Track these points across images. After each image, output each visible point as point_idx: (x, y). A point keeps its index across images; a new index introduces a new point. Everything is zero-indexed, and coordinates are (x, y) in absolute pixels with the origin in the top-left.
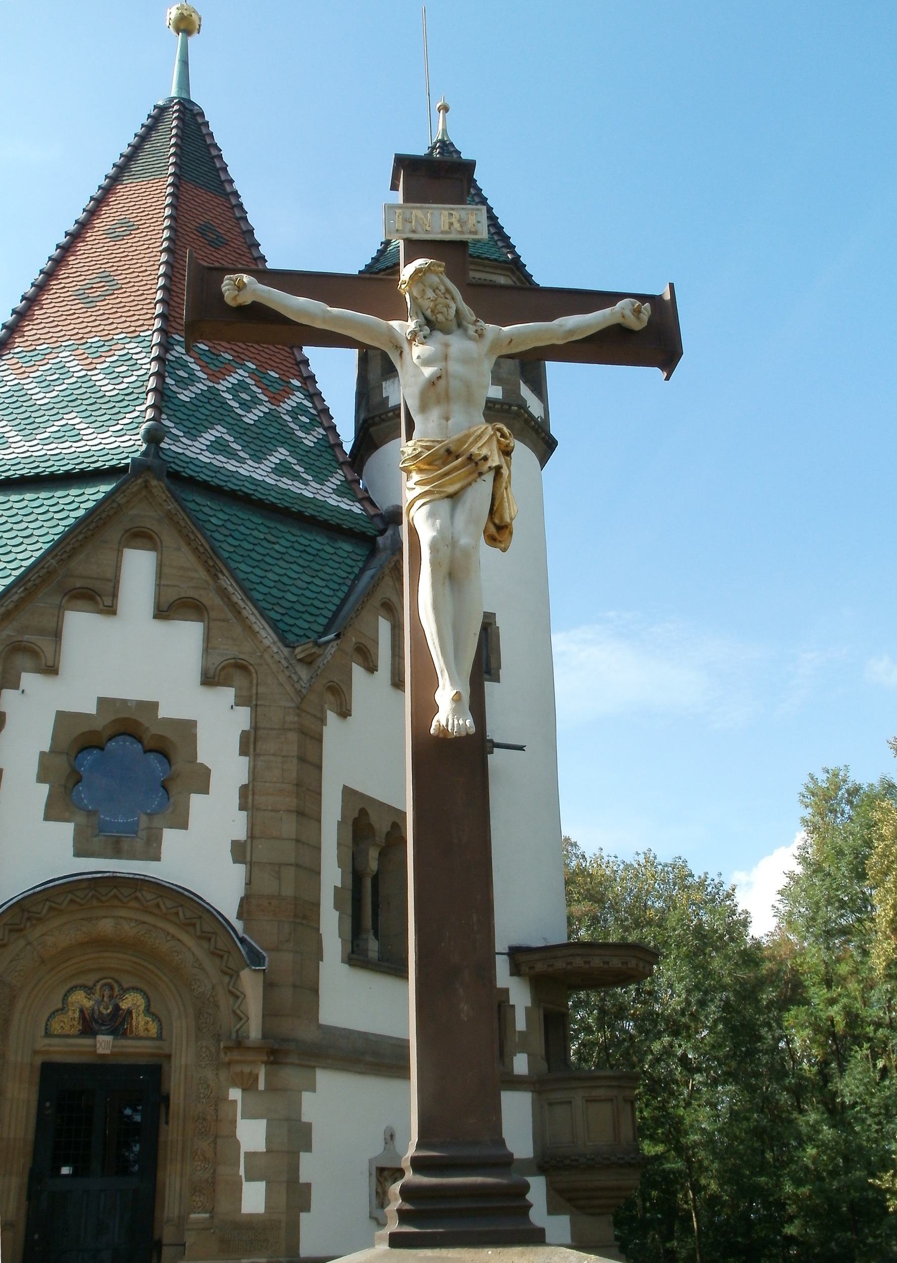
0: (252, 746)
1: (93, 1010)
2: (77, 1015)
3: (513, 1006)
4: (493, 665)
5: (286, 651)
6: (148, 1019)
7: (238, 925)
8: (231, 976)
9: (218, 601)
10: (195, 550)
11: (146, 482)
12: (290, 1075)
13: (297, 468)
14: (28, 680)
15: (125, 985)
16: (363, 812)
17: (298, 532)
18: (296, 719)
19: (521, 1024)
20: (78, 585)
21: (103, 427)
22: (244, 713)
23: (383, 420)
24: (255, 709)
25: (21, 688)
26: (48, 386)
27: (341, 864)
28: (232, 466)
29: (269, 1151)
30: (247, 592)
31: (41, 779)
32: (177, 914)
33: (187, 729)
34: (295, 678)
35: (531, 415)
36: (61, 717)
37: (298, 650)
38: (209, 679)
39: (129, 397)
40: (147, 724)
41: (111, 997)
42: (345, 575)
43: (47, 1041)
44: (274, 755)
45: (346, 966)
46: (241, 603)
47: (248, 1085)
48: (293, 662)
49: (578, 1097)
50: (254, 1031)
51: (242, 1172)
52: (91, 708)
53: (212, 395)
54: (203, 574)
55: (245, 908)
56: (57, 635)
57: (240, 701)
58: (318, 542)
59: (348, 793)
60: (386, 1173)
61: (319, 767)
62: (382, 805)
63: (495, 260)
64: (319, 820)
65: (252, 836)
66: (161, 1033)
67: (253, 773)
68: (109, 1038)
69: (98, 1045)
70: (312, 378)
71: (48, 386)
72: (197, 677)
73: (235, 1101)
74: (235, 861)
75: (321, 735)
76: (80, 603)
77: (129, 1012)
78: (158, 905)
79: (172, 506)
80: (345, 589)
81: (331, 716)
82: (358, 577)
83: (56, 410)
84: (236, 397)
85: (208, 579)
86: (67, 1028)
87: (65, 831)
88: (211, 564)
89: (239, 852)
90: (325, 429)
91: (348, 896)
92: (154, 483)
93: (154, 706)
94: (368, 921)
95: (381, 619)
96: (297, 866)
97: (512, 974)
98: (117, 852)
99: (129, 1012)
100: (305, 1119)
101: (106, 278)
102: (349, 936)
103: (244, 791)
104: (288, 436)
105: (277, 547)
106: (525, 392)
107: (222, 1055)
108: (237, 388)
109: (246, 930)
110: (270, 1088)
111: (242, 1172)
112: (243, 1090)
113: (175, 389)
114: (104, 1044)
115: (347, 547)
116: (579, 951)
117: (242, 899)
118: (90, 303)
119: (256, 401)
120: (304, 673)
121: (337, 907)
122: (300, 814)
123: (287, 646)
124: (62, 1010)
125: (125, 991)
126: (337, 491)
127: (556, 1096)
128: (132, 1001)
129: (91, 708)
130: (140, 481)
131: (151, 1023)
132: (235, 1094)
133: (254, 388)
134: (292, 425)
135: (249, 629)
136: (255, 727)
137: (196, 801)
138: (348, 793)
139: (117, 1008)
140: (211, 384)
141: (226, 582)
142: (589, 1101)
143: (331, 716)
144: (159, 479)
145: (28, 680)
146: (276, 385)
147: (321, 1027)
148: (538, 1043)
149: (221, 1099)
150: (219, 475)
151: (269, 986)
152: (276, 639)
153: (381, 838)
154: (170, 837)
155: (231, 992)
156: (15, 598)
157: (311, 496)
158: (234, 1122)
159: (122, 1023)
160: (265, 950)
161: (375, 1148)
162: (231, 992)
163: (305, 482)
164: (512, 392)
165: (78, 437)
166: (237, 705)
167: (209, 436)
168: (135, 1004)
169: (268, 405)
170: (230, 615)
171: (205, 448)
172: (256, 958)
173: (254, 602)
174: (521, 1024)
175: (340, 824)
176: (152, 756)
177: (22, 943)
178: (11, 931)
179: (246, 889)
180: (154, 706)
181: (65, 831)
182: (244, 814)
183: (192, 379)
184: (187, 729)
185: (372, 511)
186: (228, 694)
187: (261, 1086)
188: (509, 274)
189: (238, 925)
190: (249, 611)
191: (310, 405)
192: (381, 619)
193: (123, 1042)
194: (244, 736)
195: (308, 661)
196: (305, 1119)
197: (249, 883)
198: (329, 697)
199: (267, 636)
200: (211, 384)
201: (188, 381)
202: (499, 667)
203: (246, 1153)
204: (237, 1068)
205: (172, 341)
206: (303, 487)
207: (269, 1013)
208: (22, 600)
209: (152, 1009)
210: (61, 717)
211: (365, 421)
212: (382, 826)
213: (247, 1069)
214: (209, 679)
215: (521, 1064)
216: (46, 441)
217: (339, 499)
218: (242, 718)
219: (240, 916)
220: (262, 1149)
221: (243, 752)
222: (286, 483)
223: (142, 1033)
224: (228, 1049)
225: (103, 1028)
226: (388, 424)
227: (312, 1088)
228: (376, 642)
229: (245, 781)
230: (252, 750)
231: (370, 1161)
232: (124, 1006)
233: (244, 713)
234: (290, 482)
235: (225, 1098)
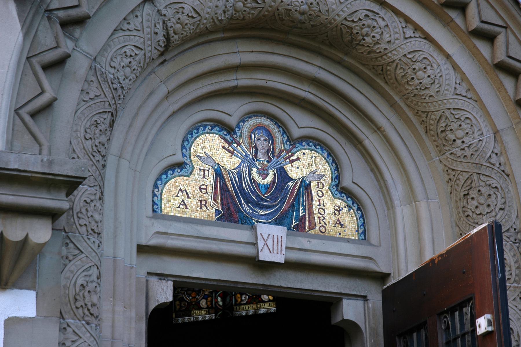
1: (240, 174)
2: (210, 181)
6: (339, 202)
15: (296, 133)
41: (270, 152)
43: (159, 226)
66: (364, 233)
68: (280, 231)
69: (261, 243)
86: (193, 202)
131: (345, 210)
159: (294, 206)
168: (314, 172)
223: (331, 229)
225: (261, 212)
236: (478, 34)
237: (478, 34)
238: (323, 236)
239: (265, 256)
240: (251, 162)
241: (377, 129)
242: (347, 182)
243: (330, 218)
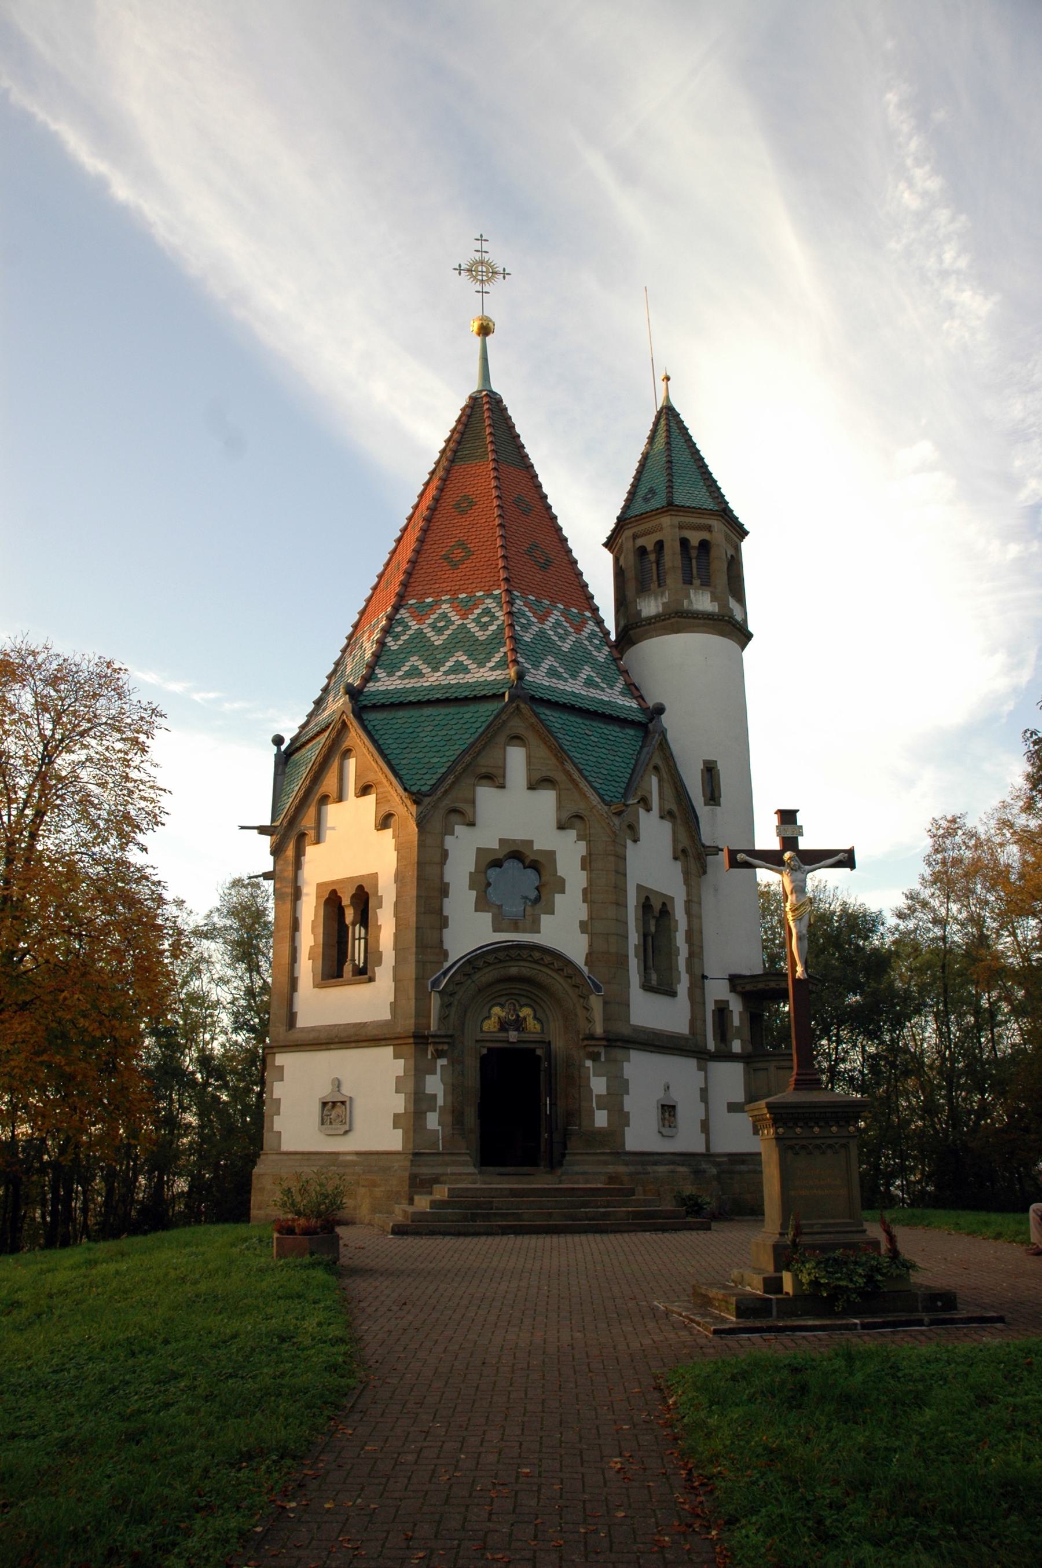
0: (588, 865)
3: (732, 1011)
4: (716, 795)
5: (606, 807)
7: (585, 969)
8: (584, 998)
9: (564, 778)
10: (549, 747)
11: (518, 706)
12: (618, 1053)
13: (597, 679)
14: (459, 829)
16: (647, 898)
17: (603, 726)
18: (612, 848)
19: (736, 1022)
20: (483, 771)
21: (481, 665)
22: (583, 844)
23: (639, 627)
24: (589, 842)
25: (456, 834)
26: (440, 631)
27: (637, 931)
28: (561, 685)
29: (608, 1094)
30: (580, 771)
31: (471, 888)
32: (553, 963)
33: (551, 855)
34: (612, 824)
35: (736, 621)
36: (480, 851)
37: (612, 808)
38: (561, 827)
39: (495, 641)
40: (527, 852)
41: (515, 1010)
42: (632, 752)
44: (602, 870)
45: (642, 990)
46: (578, 779)
47: (595, 1057)
48: (610, 814)
49: (772, 1066)
50: (599, 1030)
51: (594, 1105)
52: (496, 846)
53: (542, 634)
54: (554, 761)
55: (589, 959)
56: (473, 802)
57: (580, 838)
58: (613, 731)
59: (639, 887)
60: (666, 1108)
61: (625, 875)
62: (657, 892)
63: (711, 510)
64: (626, 907)
65: (591, 918)
67: (590, 881)
68: (515, 1033)
70: (597, 609)
71: (440, 631)
72: (554, 824)
73: (589, 1068)
74: (582, 932)
75: (625, 856)
76: (484, 781)
77: (525, 1019)
78: (542, 959)
79: (534, 720)
80: (633, 762)
81: (629, 843)
82: (639, 753)
83: (450, 647)
84: (556, 634)
85: (558, 764)
87: (487, 917)
88: (559, 755)
89: (584, 927)
90: (609, 647)
91: (642, 949)
92: (522, 706)
93: (531, 842)
94: (650, 963)
95: (653, 777)
96: (617, 935)
97: (731, 991)
98: (516, 929)
99: (525, 1019)
100: (625, 1077)
101: (462, 545)
102: (643, 974)
103: (585, 891)
104: (588, 656)
105: (592, 738)
106: (733, 604)
107: (580, 1042)
108: (556, 625)
109: (590, 972)
110: (607, 1060)
111: (594, 1105)
112: (594, 1061)
113: (521, 633)
114: (513, 1036)
115: (632, 732)
116: (774, 978)
117: (587, 955)
118: (455, 566)
119: (568, 634)
120: (616, 821)
121: (636, 956)
122: (617, 904)
123: (606, 805)
124: (489, 1017)
125: (521, 1006)
126: (622, 693)
127: (760, 1065)
128: (526, 1012)
129: (496, 846)
130: (514, 705)
132: (589, 1063)
133: (565, 624)
134: (590, 647)
135: (584, 795)
136: (590, 853)
137: (558, 898)
138: (639, 887)
139: (518, 1016)
140: (540, 626)
141: (569, 767)
142: (778, 1068)
143: (629, 843)
144: (526, 703)
145: (459, 829)
146: (576, 618)
147: (631, 1025)
148: (746, 1032)
149: (582, 1066)
150: (555, 694)
151: (606, 1003)
152: (600, 801)
153: (657, 914)
154: (545, 919)
155: (584, 1007)
156: (450, 782)
157: (608, 699)
158: (589, 1078)
160: (602, 983)
161: (660, 1094)
162: (584, 1007)
163: (603, 689)
164: (724, 605)
165: (466, 670)
166: (578, 840)
167: (545, 666)
169: (574, 635)
170: (571, 786)
171: (544, 675)
172: (598, 988)
173: (585, 778)
174: (736, 1022)
175: (636, 906)
176: (529, 871)
177: (470, 981)
178: (464, 975)
179: (589, 949)
180: (531, 842)
181: (487, 917)
182: (586, 904)
183: (530, 624)
184: (551, 855)
185: (645, 706)
186: (572, 834)
187: (603, 1059)
188: (720, 518)
189: (585, 969)
190: (583, 784)
191: (598, 630)
192: (653, 777)
193: (523, 1035)
194: (583, 859)
195: (619, 814)
196: (625, 1077)
197: (591, 946)
198: (628, 831)
199: (595, 799)
200: (540, 626)
201: (527, 626)
202: (720, 796)
203: (596, 1096)
204: (591, 1049)
205: (515, 597)
206: (602, 693)
207: (607, 1019)
208: (453, 783)
209: (537, 1016)
210: (480, 851)
211: (626, 626)
212: (657, 906)
213: (596, 1050)
214: (561, 827)
215: (737, 1046)
216: (446, 673)
217: (623, 699)
218: (582, 848)
219: (586, 964)
220: (605, 1093)
221: (583, 868)
222: (594, 693)
223: (532, 1030)
224: (583, 1040)
226: (642, 629)
227: (628, 1060)
228: (651, 793)
229: (585, 885)
230: (588, 868)
231: (658, 1101)
232: (521, 1015)
233: (583, 844)
234: (594, 691)
235: (584, 1066)
236: (567, 977)
237: (567, 977)
238: (530, 1033)
239: (511, 1040)
240: (508, 1013)
241: (545, 1002)
242: (537, 1016)
243: (532, 1026)
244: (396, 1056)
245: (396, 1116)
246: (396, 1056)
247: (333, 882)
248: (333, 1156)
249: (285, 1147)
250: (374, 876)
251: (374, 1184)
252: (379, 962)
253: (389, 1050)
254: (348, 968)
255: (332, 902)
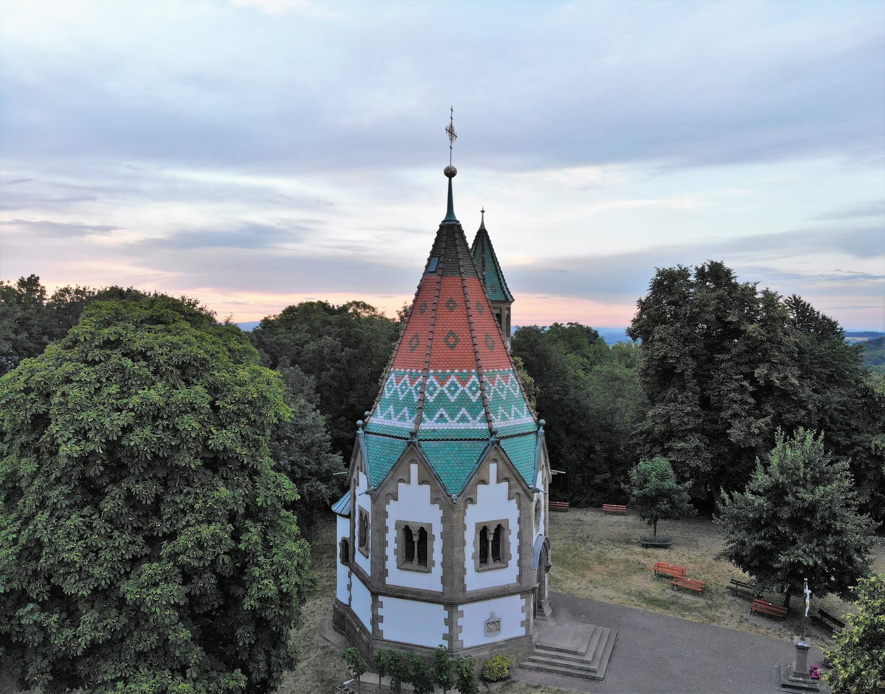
244: (522, 598)
245: (522, 622)
246: (522, 598)
247: (485, 523)
248: (495, 645)
249: (466, 646)
250: (507, 521)
251: (518, 652)
252: (510, 559)
253: (519, 596)
254: (490, 559)
255: (483, 532)
